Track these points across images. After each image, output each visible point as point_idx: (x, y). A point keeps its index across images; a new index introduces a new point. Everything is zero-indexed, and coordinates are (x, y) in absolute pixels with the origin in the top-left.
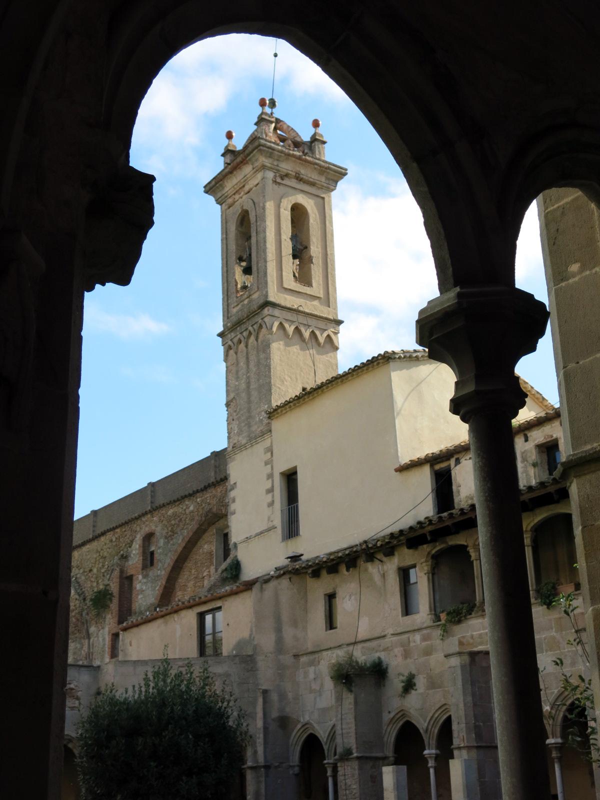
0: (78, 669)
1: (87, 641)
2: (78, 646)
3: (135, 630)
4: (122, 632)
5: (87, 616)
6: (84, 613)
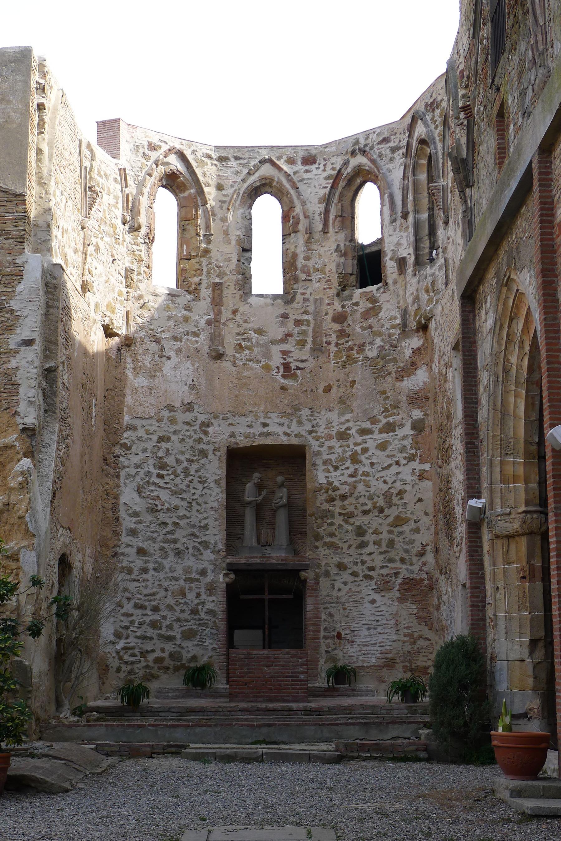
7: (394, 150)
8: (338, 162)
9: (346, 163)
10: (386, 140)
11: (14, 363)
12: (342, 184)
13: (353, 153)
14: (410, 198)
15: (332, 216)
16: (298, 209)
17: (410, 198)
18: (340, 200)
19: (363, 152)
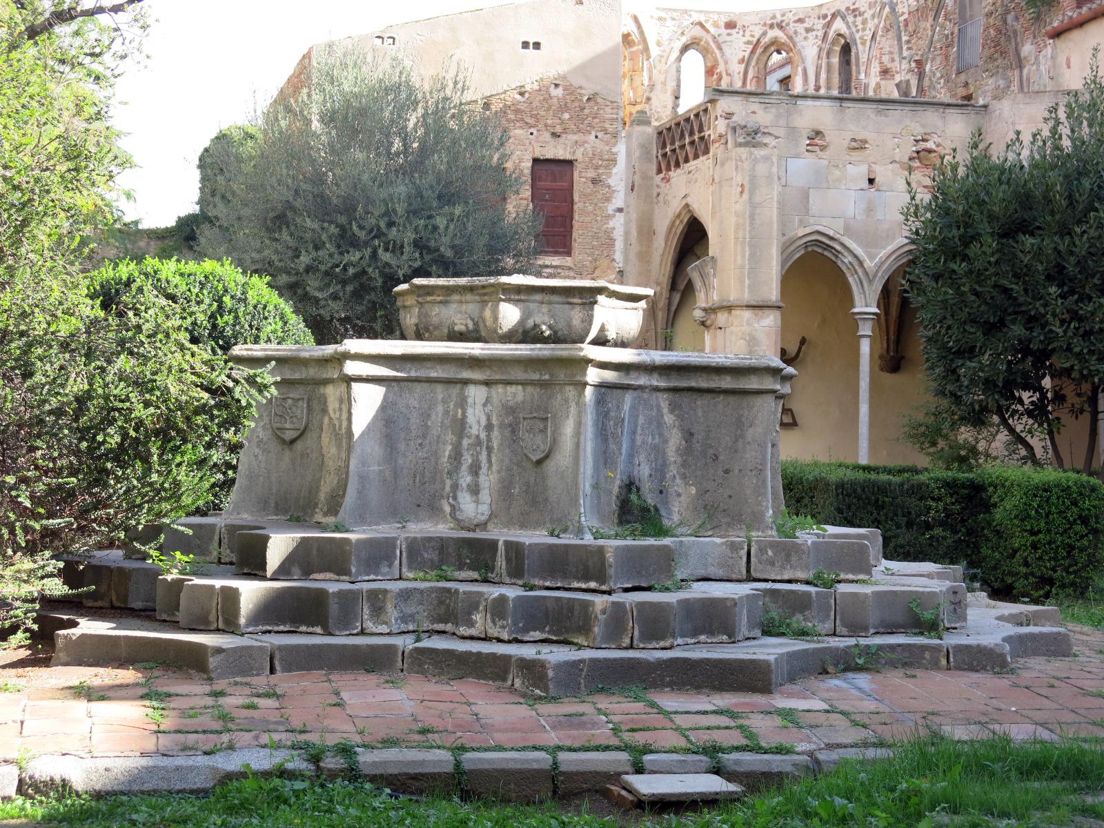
0: (941, 110)
1: (1017, 72)
2: (1002, 83)
3: (1076, 35)
4: (1051, 41)
5: (1015, 23)
6: (1010, 18)
7: (808, 30)
8: (758, 32)
9: (765, 34)
10: (800, 21)
11: (611, 224)
12: (759, 50)
13: (771, 26)
14: (823, 76)
15: (750, 76)
16: (721, 68)
17: (823, 76)
18: (757, 63)
19: (780, 27)
